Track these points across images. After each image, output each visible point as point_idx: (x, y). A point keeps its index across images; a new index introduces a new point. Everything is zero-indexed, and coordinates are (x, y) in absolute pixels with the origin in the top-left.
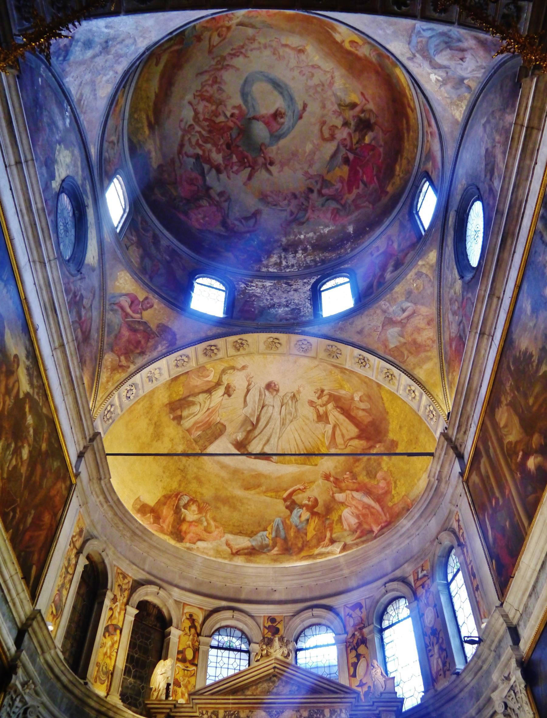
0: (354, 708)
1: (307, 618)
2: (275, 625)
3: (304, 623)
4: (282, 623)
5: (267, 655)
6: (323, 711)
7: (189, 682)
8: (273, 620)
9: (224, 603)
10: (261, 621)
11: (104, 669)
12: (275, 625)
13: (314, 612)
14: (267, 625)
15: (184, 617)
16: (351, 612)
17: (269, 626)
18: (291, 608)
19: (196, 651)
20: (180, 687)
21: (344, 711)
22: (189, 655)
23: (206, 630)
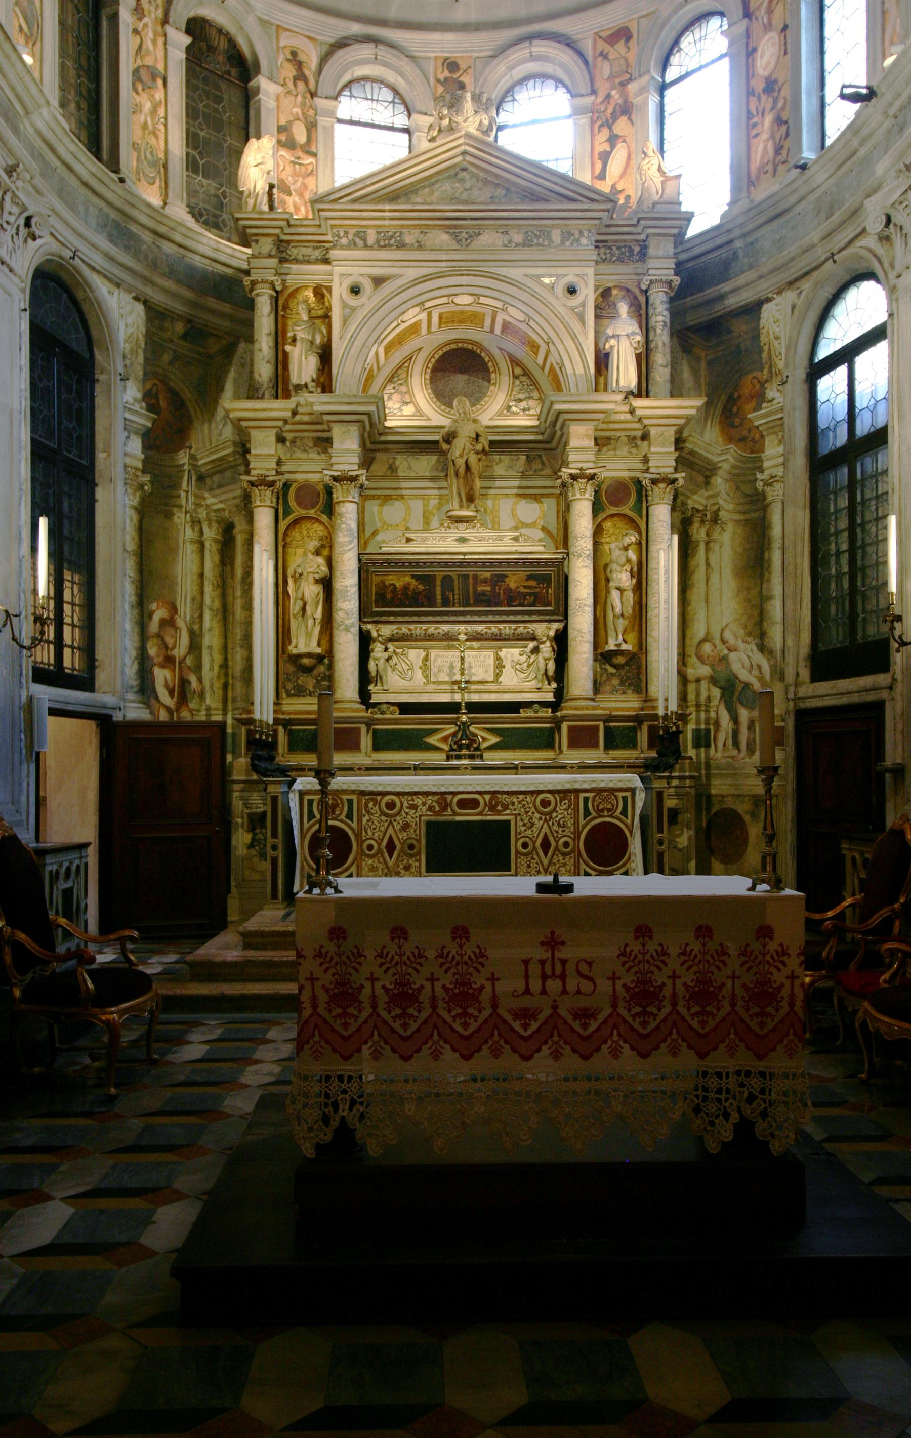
0: (604, 230)
1: (520, 61)
2: (455, 76)
3: (514, 72)
4: (470, 71)
5: (451, 129)
6: (549, 233)
7: (305, 186)
8: (452, 66)
9: (356, 28)
10: (430, 67)
11: (148, 155)
12: (455, 76)
13: (534, 49)
14: (442, 77)
15: (281, 58)
16: (607, 48)
17: (446, 79)
18: (486, 41)
19: (311, 127)
20: (290, 194)
21: (586, 233)
22: (300, 134)
23: (325, 87)
